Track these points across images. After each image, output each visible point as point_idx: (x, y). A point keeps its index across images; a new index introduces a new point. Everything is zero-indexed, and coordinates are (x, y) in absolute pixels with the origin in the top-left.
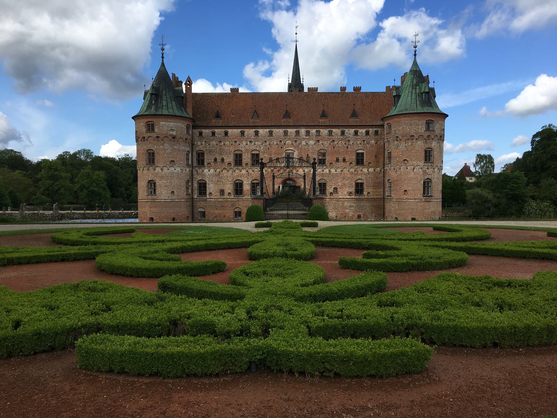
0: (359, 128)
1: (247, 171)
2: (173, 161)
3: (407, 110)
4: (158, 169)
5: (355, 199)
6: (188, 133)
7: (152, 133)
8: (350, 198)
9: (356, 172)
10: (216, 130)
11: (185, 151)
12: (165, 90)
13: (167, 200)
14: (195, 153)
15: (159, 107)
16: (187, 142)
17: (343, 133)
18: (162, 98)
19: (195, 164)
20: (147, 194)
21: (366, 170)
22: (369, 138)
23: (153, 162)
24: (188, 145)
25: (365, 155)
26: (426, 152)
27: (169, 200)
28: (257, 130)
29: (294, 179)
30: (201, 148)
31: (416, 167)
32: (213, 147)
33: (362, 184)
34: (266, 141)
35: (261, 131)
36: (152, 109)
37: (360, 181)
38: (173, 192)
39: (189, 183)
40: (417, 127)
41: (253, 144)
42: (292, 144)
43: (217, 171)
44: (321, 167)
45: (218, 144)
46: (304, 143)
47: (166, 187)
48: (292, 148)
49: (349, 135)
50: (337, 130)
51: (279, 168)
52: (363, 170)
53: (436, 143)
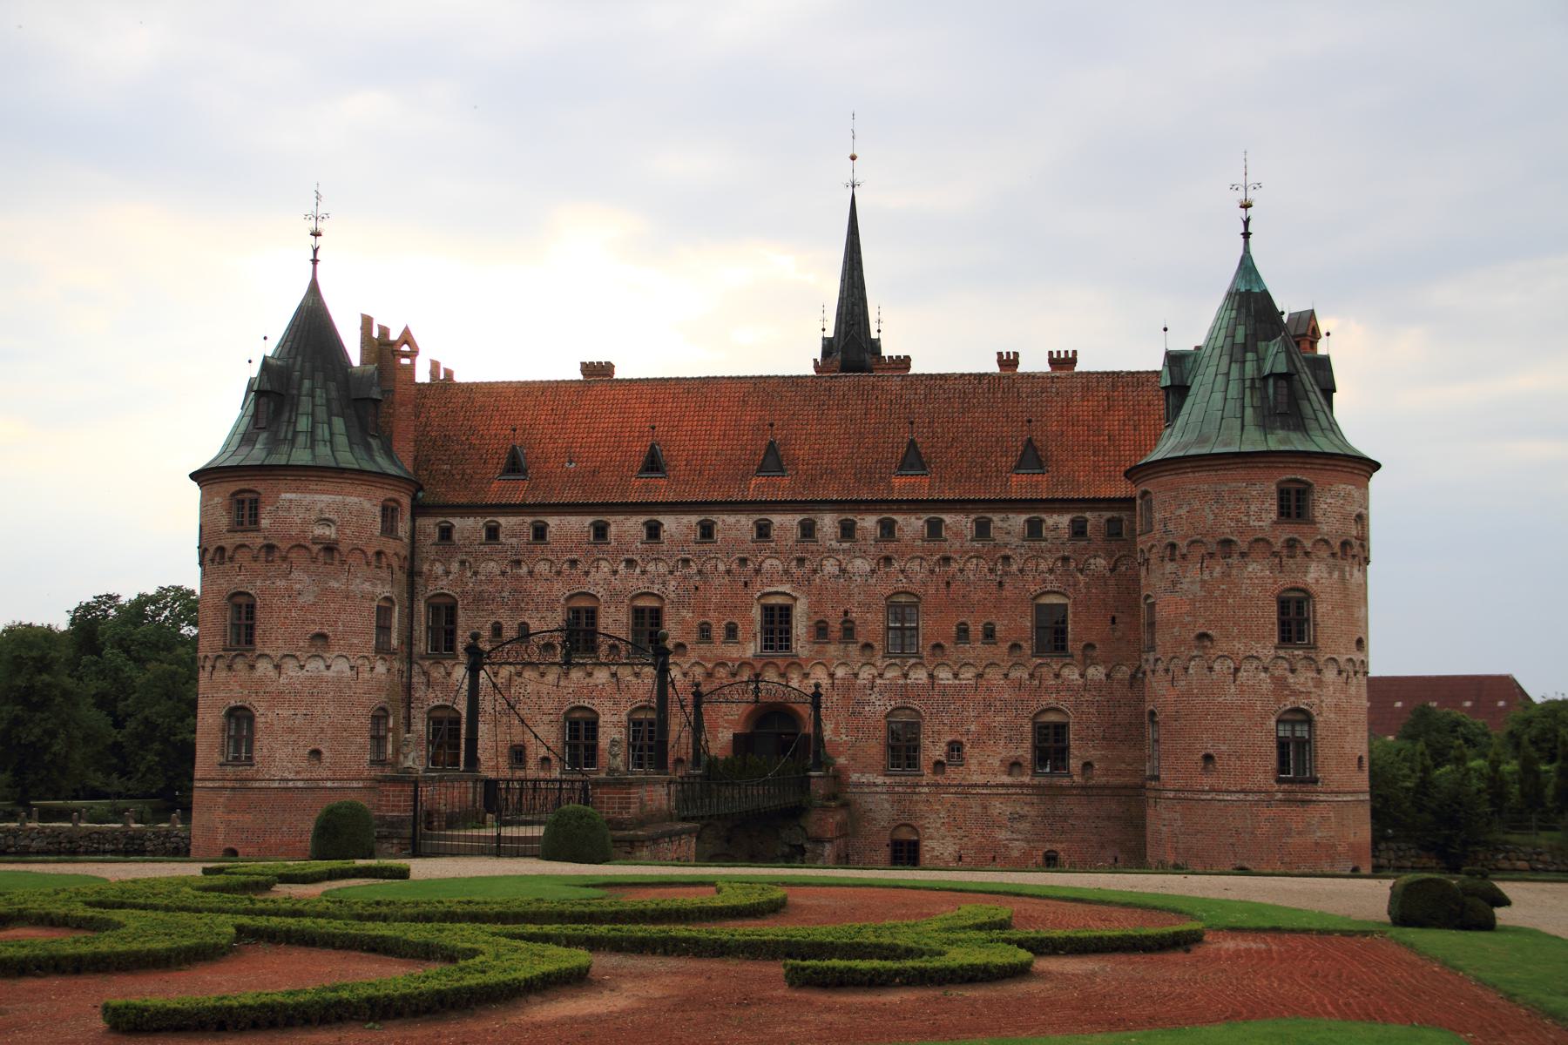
0: (1046, 511)
1: (614, 675)
2: (322, 636)
3: (1202, 440)
4: (264, 667)
5: (1034, 787)
6: (389, 530)
7: (251, 534)
8: (1013, 786)
9: (1037, 682)
10: (502, 520)
11: (373, 600)
12: (312, 378)
13: (291, 784)
14: (421, 606)
15: (282, 436)
16: (384, 564)
17: (983, 529)
18: (295, 406)
19: (421, 646)
20: (222, 760)
21: (1077, 671)
22: (1086, 548)
23: (250, 641)
24: (384, 574)
25: (1070, 616)
26: (1283, 604)
27: (300, 784)
28: (655, 517)
29: (795, 706)
30: (444, 585)
31: (1246, 665)
32: (491, 582)
33: (1060, 730)
34: (686, 561)
35: (669, 523)
36: (258, 446)
37: (1052, 718)
38: (316, 753)
39: (387, 717)
40: (1243, 507)
41: (638, 570)
42: (786, 572)
43: (500, 675)
44: (898, 661)
45: (509, 570)
46: (830, 567)
47: (292, 731)
48: (786, 588)
49: (1007, 539)
50: (960, 517)
51: (737, 664)
52: (1066, 672)
53: (1323, 567)
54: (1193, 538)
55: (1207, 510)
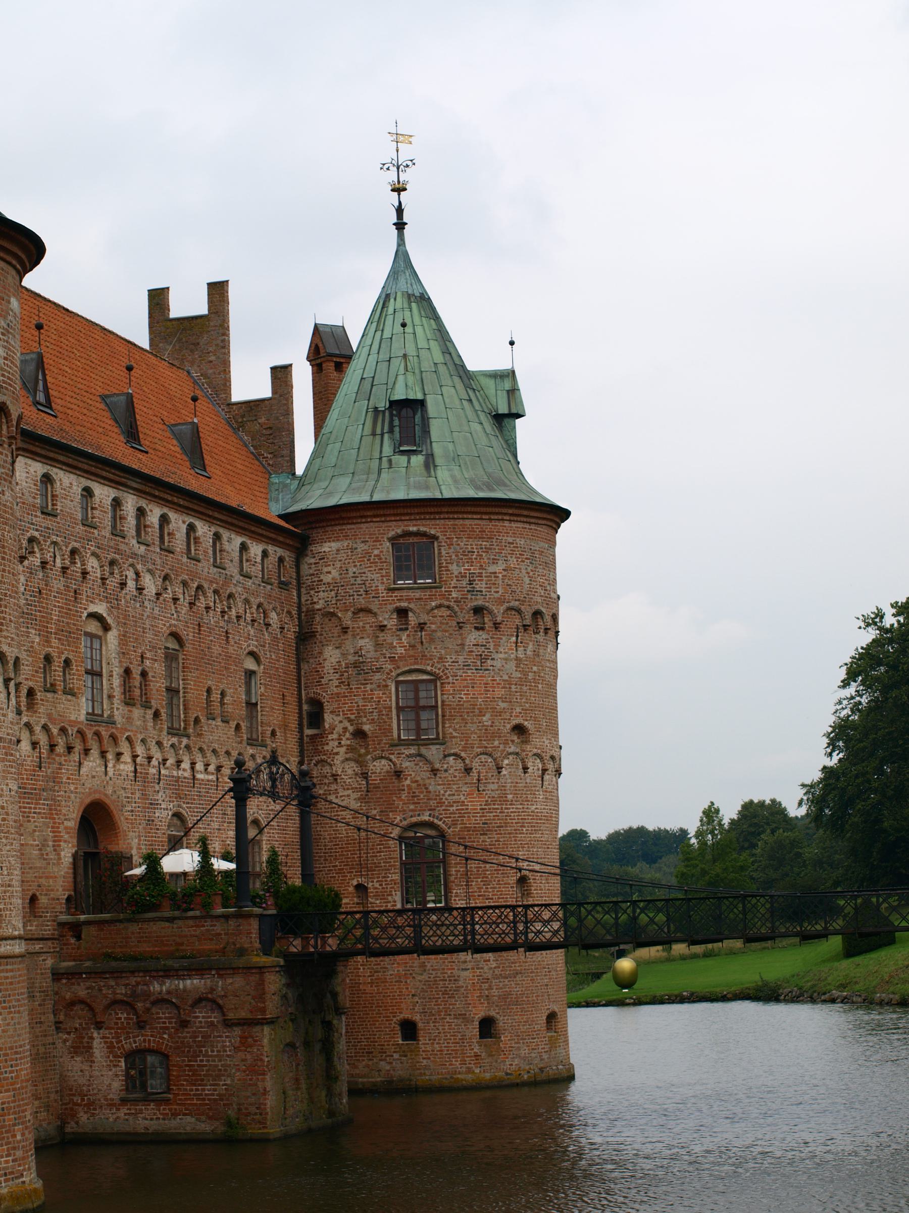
48: (100, 608)
54: (511, 604)
55: (524, 571)
